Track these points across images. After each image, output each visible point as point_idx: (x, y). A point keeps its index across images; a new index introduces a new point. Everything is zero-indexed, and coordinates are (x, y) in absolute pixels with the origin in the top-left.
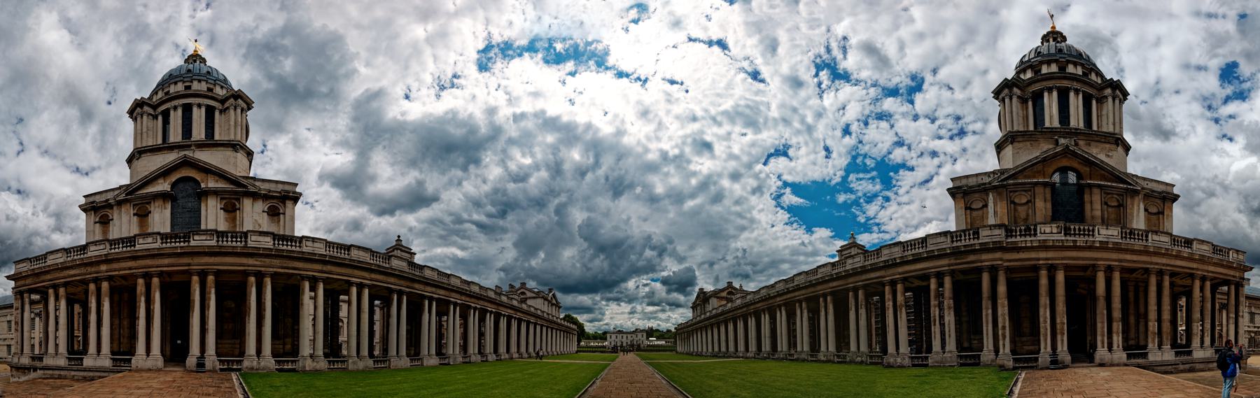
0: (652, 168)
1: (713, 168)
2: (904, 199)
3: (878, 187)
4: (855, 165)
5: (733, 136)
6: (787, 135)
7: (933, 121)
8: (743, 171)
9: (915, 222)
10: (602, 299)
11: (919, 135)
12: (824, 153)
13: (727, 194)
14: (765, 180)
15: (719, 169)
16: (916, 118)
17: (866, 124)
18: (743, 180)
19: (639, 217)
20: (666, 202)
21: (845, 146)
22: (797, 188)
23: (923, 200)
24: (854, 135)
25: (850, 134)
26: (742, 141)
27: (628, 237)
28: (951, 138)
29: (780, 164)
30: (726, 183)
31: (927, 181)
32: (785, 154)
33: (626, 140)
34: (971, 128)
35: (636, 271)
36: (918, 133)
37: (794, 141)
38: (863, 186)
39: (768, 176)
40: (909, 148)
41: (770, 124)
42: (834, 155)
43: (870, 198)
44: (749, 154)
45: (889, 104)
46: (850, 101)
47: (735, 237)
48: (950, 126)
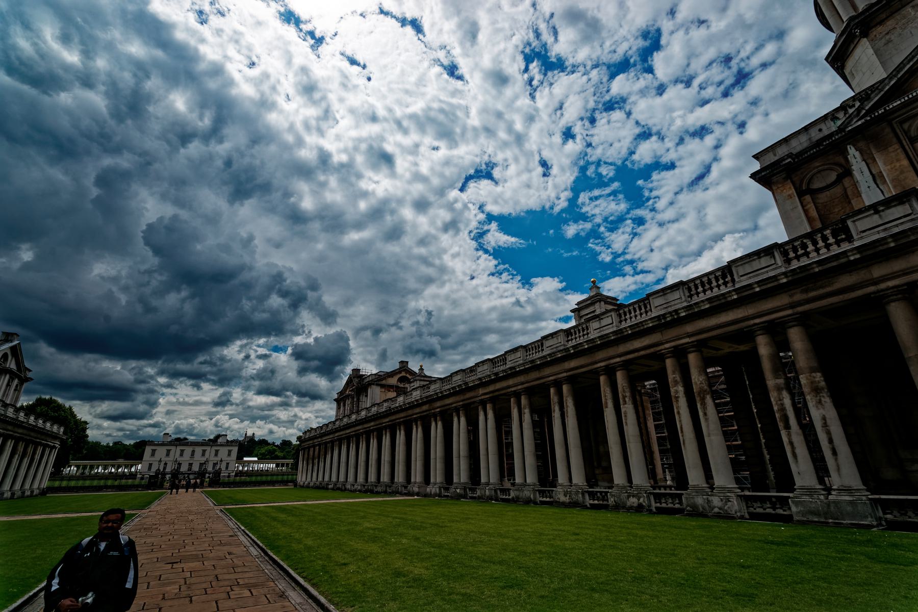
0: (304, 171)
1: (391, 189)
2: (669, 214)
3: (623, 206)
4: (586, 179)
5: (422, 149)
6: (490, 150)
7: (688, 83)
8: (432, 198)
9: (694, 247)
10: (162, 373)
11: (673, 110)
12: (540, 170)
13: (408, 228)
14: (461, 212)
15: (399, 193)
16: (661, 90)
17: (593, 121)
18: (432, 211)
19: (269, 241)
20: (316, 226)
21: (568, 156)
22: (506, 223)
23: (701, 209)
24: (579, 138)
25: (573, 137)
26: (432, 158)
27: (242, 268)
28: (726, 94)
29: (481, 189)
30: (408, 213)
31: (701, 177)
32: (489, 176)
33: (272, 118)
34: (755, 61)
35: (247, 329)
36: (671, 110)
37: (499, 157)
38: (602, 207)
39: (465, 206)
40: (662, 138)
41: (469, 135)
42: (555, 171)
43: (614, 224)
44: (441, 175)
45: (620, 85)
46: (570, 93)
47: (416, 293)
48: (718, 79)
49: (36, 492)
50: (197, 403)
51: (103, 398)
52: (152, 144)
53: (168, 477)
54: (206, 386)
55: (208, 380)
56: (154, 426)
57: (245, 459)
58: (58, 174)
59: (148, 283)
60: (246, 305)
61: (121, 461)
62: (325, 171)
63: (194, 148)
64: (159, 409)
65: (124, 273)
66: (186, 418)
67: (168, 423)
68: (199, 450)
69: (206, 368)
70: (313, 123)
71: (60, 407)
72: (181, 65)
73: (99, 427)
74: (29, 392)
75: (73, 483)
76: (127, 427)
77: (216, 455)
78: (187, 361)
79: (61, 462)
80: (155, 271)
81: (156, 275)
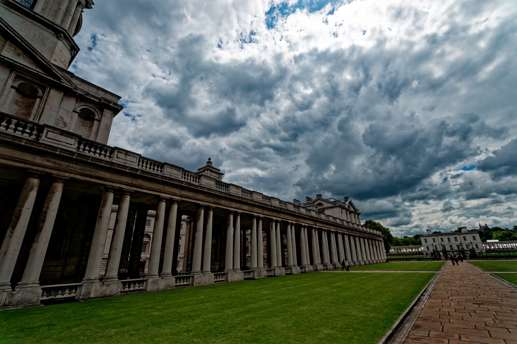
0: (424, 57)
10: (404, 200)
19: (424, 109)
20: (452, 81)
27: (417, 132)
33: (388, 46)
49: (384, 261)
50: (434, 212)
51: (386, 217)
52: (347, 101)
53: (441, 253)
54: (431, 201)
55: (431, 198)
56: (417, 227)
57: (488, 241)
58: (327, 135)
59: (375, 162)
60: (429, 150)
61: (411, 246)
62: (437, 47)
63: (363, 90)
64: (414, 218)
65: (365, 160)
66: (432, 221)
67: (423, 225)
68: (452, 238)
69: (426, 193)
70: (412, 28)
71: (375, 224)
72: (337, 60)
73: (392, 231)
74: (362, 219)
75: (395, 257)
76: (404, 229)
77: (465, 239)
78: (412, 191)
79: (387, 249)
80: (375, 155)
81: (376, 156)
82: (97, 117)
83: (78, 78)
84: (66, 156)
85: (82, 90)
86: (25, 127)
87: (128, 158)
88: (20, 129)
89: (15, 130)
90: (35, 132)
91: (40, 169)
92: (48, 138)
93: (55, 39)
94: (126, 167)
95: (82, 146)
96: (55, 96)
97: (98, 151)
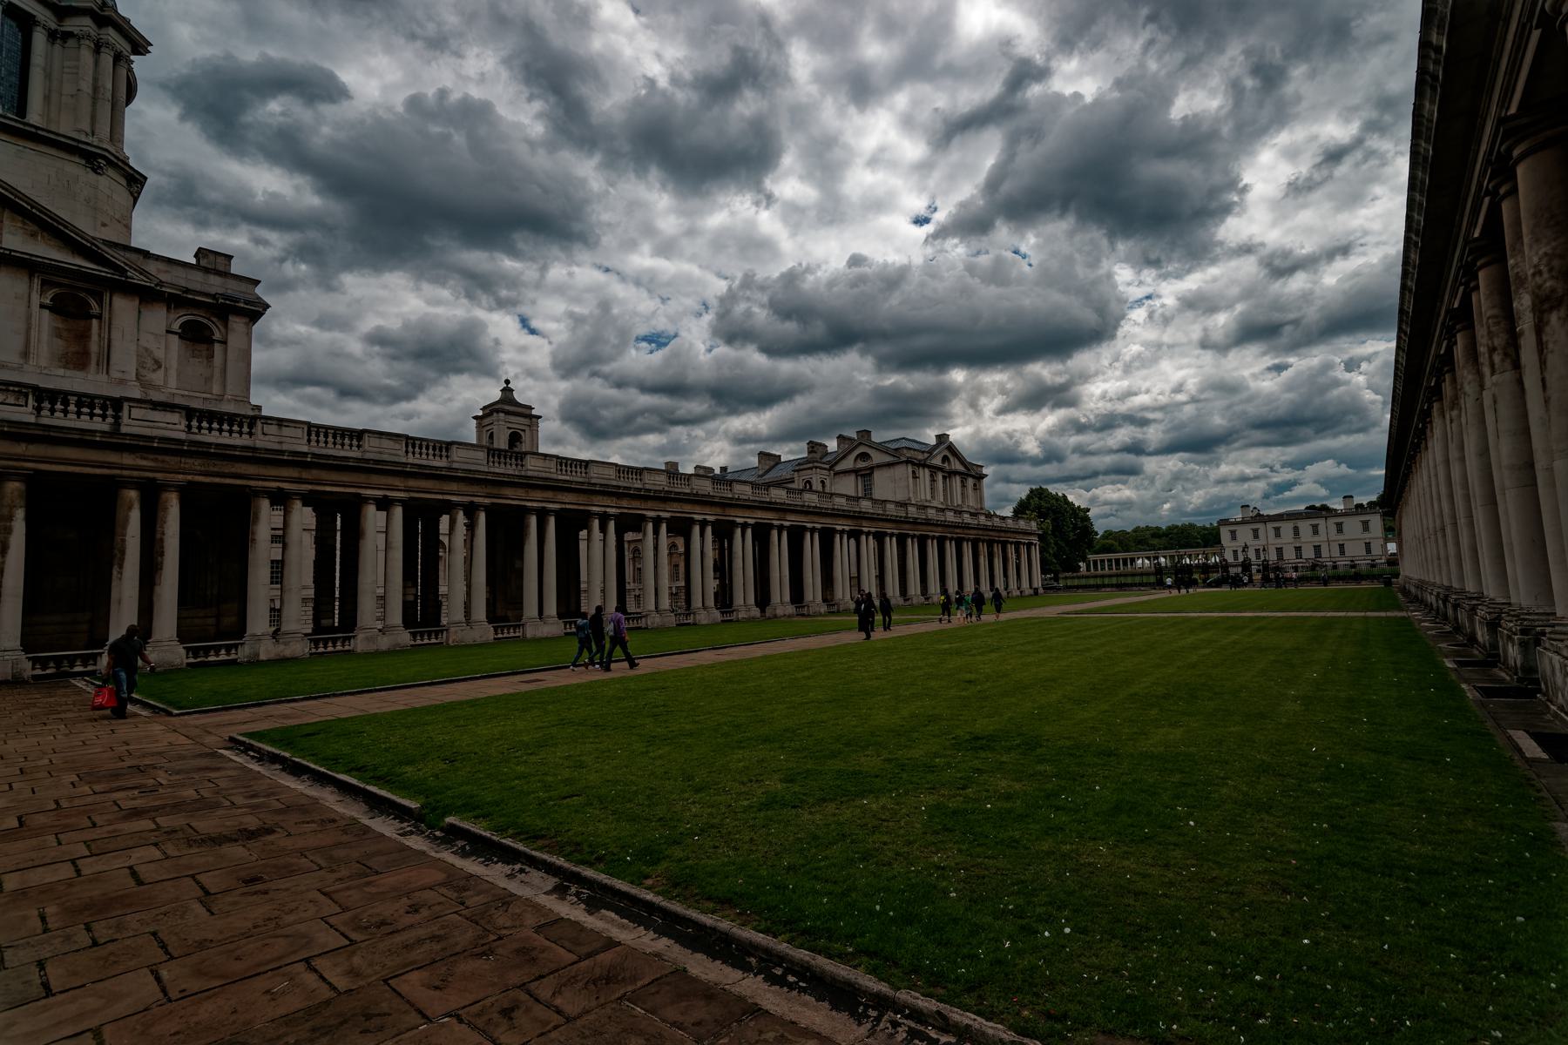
82: (217, 336)
83: (158, 258)
84: (171, 448)
85: (173, 285)
86: (92, 406)
87: (286, 431)
88: (85, 410)
89: (79, 414)
90: (110, 412)
91: (135, 473)
92: (134, 422)
93: (92, 176)
94: (282, 452)
95: (195, 423)
96: (124, 308)
97: (226, 427)
